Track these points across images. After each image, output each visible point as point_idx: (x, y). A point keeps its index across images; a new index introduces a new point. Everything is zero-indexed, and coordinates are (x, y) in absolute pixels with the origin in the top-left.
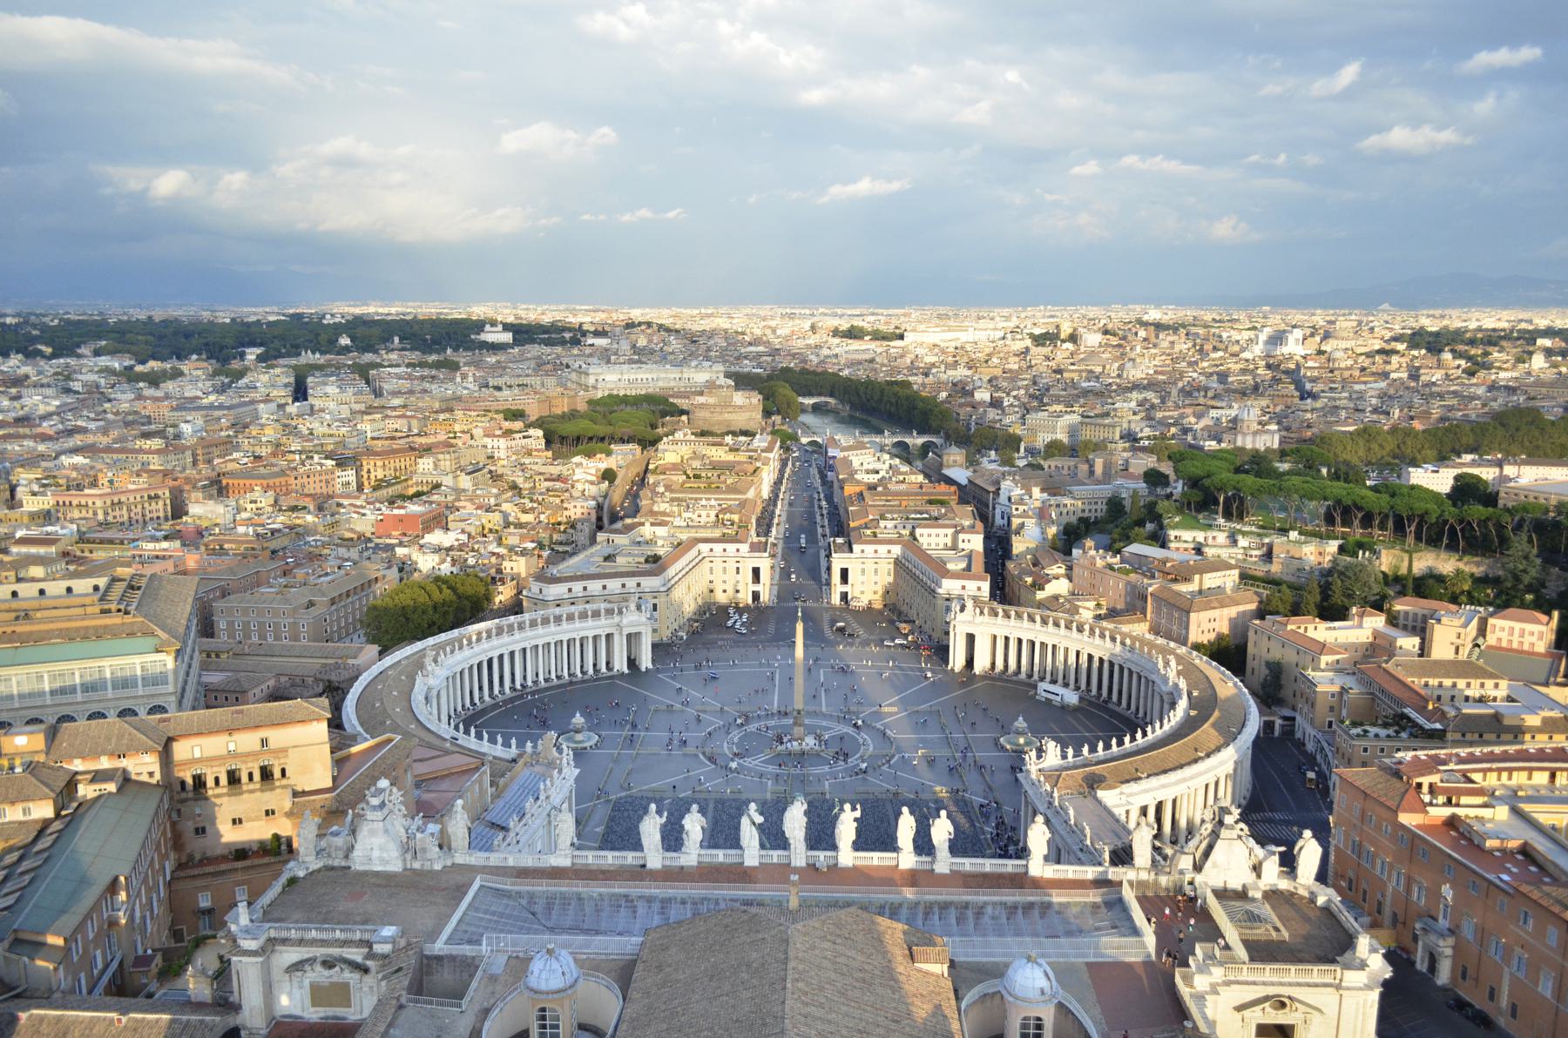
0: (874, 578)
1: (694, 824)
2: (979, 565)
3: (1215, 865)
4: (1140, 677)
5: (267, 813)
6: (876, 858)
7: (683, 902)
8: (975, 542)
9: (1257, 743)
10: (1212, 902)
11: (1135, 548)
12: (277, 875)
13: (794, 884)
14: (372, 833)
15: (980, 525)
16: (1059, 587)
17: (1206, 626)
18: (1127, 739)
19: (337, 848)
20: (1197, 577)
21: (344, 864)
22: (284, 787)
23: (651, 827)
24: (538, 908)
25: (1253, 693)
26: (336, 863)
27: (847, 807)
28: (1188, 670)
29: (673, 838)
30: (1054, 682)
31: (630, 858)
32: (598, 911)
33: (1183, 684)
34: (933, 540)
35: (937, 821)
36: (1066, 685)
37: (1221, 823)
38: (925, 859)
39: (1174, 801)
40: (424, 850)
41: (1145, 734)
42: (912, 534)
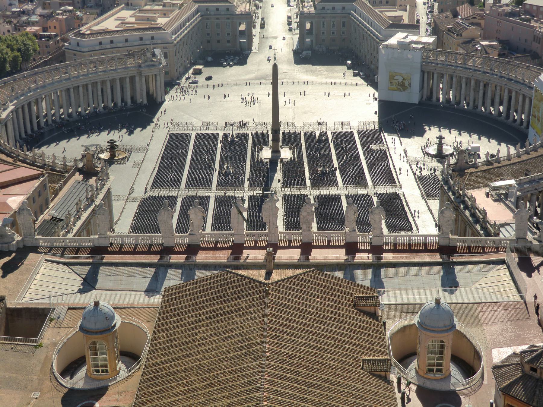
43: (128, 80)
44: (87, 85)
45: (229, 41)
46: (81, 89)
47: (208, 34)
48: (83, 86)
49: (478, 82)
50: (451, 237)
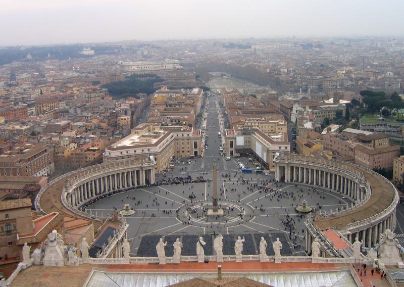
1: (178, 246)
3: (386, 256)
5: (9, 243)
6: (251, 257)
8: (285, 130)
9: (397, 207)
11: (348, 130)
12: (16, 268)
13: (220, 269)
14: (51, 251)
16: (317, 146)
17: (376, 161)
20: (373, 141)
22: (16, 234)
23: (161, 247)
26: (38, 263)
27: (239, 237)
29: (169, 251)
31: (152, 259)
33: (368, 184)
34: (267, 129)
35: (276, 242)
38: (271, 257)
40: (71, 257)
41: (354, 204)
43: (136, 172)
44: (114, 175)
45: (189, 152)
46: (111, 177)
48: (112, 176)
49: (322, 172)
50: (320, 258)
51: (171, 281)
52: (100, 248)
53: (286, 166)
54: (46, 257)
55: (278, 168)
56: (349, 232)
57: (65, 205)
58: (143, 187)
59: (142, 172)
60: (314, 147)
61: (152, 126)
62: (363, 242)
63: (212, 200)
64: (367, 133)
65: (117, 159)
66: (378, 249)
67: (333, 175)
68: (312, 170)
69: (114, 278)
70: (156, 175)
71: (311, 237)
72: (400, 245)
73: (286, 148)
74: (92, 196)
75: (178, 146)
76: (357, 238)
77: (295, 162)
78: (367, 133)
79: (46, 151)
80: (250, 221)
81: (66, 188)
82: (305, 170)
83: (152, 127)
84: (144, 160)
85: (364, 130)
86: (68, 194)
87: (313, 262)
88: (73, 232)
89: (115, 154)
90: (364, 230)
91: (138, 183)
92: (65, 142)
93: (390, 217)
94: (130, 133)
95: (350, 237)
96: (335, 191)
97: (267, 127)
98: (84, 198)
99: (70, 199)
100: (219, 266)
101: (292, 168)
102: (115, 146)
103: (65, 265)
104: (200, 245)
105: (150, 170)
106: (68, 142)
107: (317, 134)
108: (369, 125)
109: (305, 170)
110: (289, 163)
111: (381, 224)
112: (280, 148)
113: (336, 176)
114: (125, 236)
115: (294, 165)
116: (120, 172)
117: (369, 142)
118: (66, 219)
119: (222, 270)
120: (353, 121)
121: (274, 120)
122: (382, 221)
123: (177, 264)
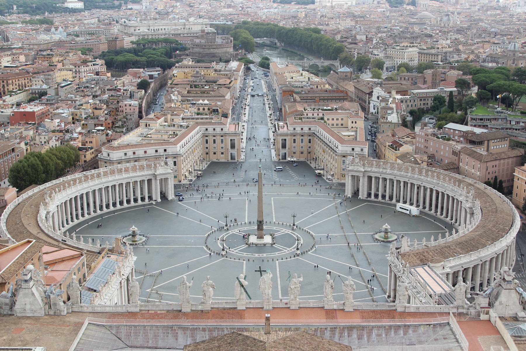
0: (302, 145)
2: (361, 136)
3: (501, 303)
4: (453, 199)
7: (204, 330)
8: (361, 124)
9: (521, 235)
10: (500, 325)
11: (451, 126)
13: (268, 319)
14: (26, 295)
15: (361, 114)
16: (406, 148)
17: (490, 170)
18: (447, 234)
19: (6, 304)
20: (486, 142)
21: (10, 313)
24: (123, 336)
25: (517, 207)
28: (479, 194)
30: (405, 202)
32: (156, 336)
34: (335, 122)
36: (411, 204)
37: (504, 279)
39: (473, 268)
40: (55, 304)
41: (457, 232)
42: (322, 119)
43: (146, 182)
44: (115, 186)
45: (222, 153)
46: (110, 189)
47: (207, 148)
51: (198, 336)
52: (95, 291)
53: (361, 175)
54: (17, 303)
55: (350, 178)
56: (448, 270)
57: (43, 228)
58: (157, 204)
59: (156, 182)
60: (401, 149)
61: (169, 116)
62: (469, 282)
63: (256, 222)
64: (478, 131)
65: (119, 163)
66: (490, 294)
67: (428, 190)
68: (399, 182)
69: (117, 332)
70: (176, 187)
71: (395, 275)
72: (521, 289)
73: (362, 150)
74: (83, 215)
75: (207, 145)
76: (460, 278)
77: (375, 169)
78: (478, 131)
79: (13, 150)
80: (309, 253)
81: (46, 204)
82: (388, 181)
83: (169, 116)
84: (158, 165)
85: (475, 126)
86: (48, 213)
87: (399, 310)
88: (55, 267)
89: (116, 155)
90: (469, 268)
91: (150, 198)
92: (43, 137)
93: (507, 250)
94: (138, 126)
95: (451, 277)
96: (429, 212)
97: (335, 119)
98: (72, 218)
99: (51, 219)
100: (266, 315)
101: (370, 178)
102: (115, 143)
103: (46, 315)
104: (239, 285)
105: (166, 179)
106: (47, 138)
107: (408, 131)
108: (481, 119)
109: (388, 181)
110: (365, 171)
111: (495, 259)
112: (353, 149)
113: (431, 190)
114: (132, 273)
115: (373, 175)
116: (124, 182)
117: (480, 143)
118: (46, 249)
119: (271, 320)
120: (459, 113)
121: (346, 110)
122: (496, 255)
123: (208, 312)
